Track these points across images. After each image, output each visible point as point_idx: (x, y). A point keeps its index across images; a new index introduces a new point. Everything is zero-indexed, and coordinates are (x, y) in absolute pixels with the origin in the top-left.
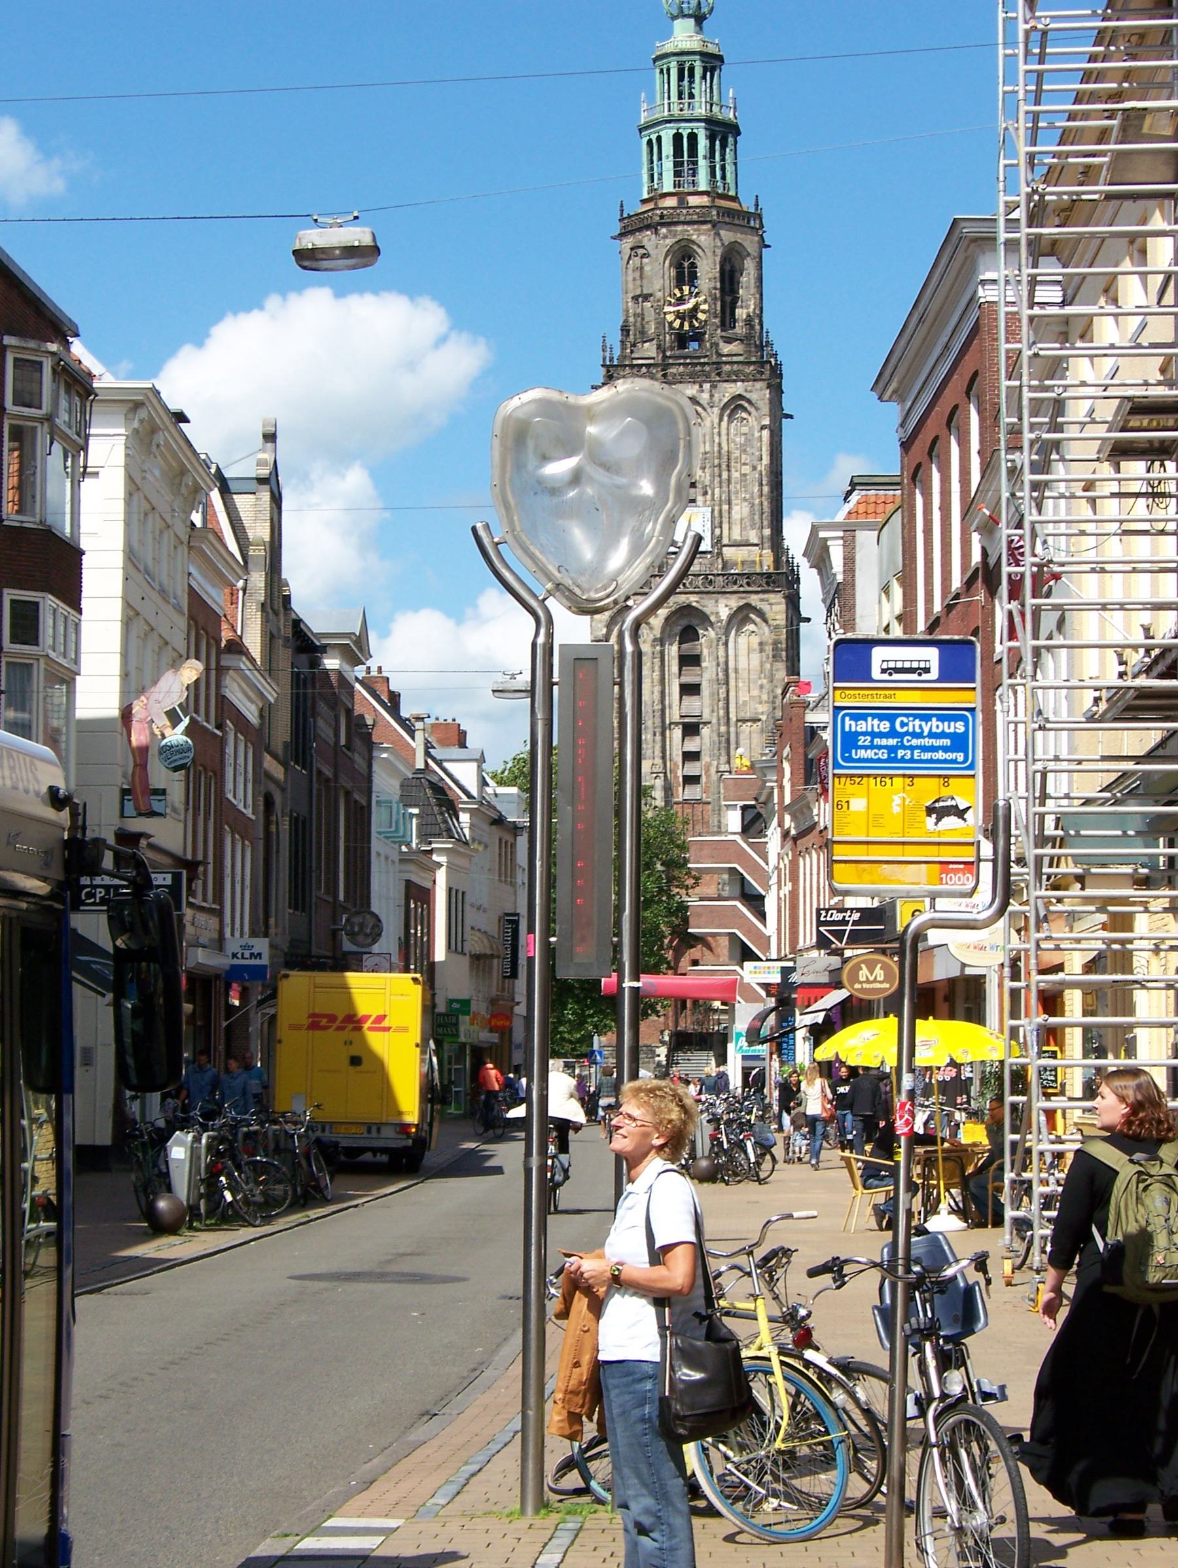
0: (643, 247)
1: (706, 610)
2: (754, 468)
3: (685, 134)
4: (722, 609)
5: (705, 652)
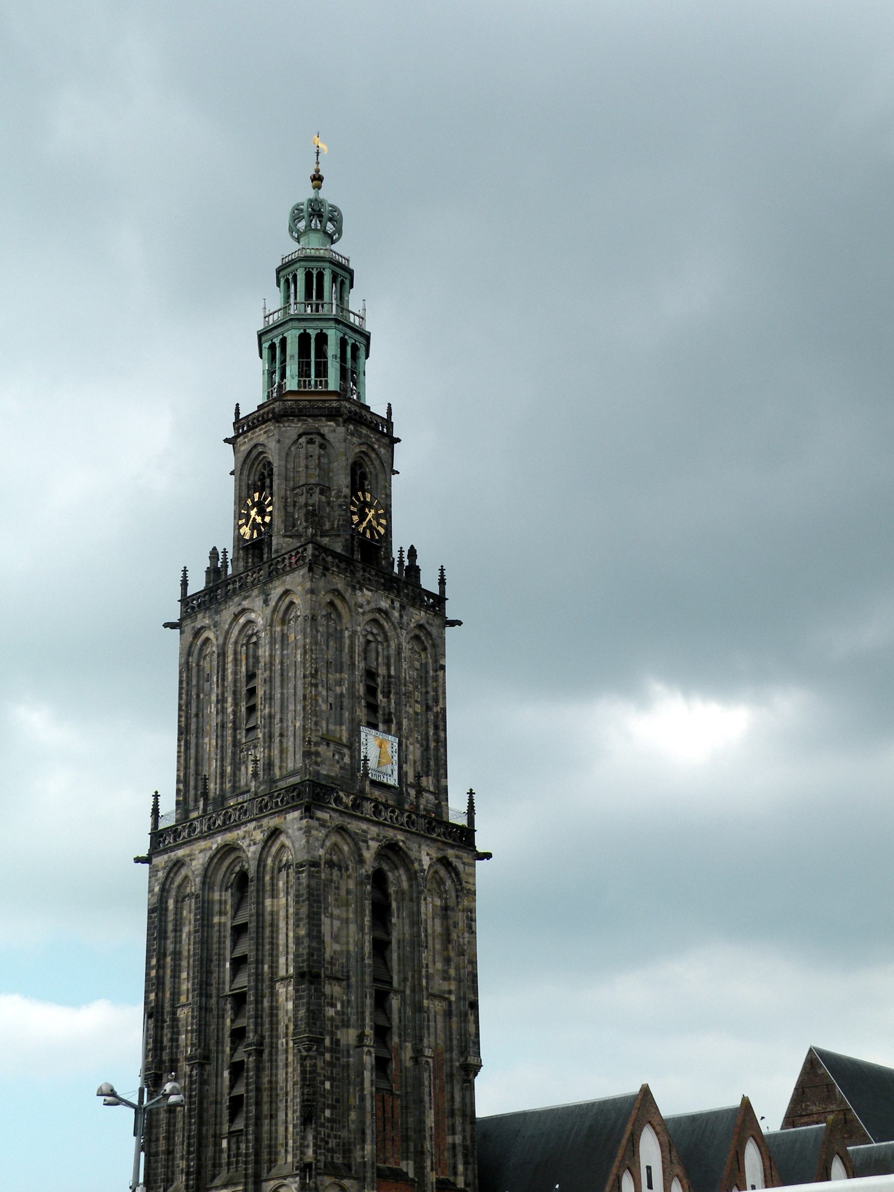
0: (322, 436)
1: (410, 853)
2: (428, 708)
3: (350, 341)
4: (425, 856)
5: (394, 905)
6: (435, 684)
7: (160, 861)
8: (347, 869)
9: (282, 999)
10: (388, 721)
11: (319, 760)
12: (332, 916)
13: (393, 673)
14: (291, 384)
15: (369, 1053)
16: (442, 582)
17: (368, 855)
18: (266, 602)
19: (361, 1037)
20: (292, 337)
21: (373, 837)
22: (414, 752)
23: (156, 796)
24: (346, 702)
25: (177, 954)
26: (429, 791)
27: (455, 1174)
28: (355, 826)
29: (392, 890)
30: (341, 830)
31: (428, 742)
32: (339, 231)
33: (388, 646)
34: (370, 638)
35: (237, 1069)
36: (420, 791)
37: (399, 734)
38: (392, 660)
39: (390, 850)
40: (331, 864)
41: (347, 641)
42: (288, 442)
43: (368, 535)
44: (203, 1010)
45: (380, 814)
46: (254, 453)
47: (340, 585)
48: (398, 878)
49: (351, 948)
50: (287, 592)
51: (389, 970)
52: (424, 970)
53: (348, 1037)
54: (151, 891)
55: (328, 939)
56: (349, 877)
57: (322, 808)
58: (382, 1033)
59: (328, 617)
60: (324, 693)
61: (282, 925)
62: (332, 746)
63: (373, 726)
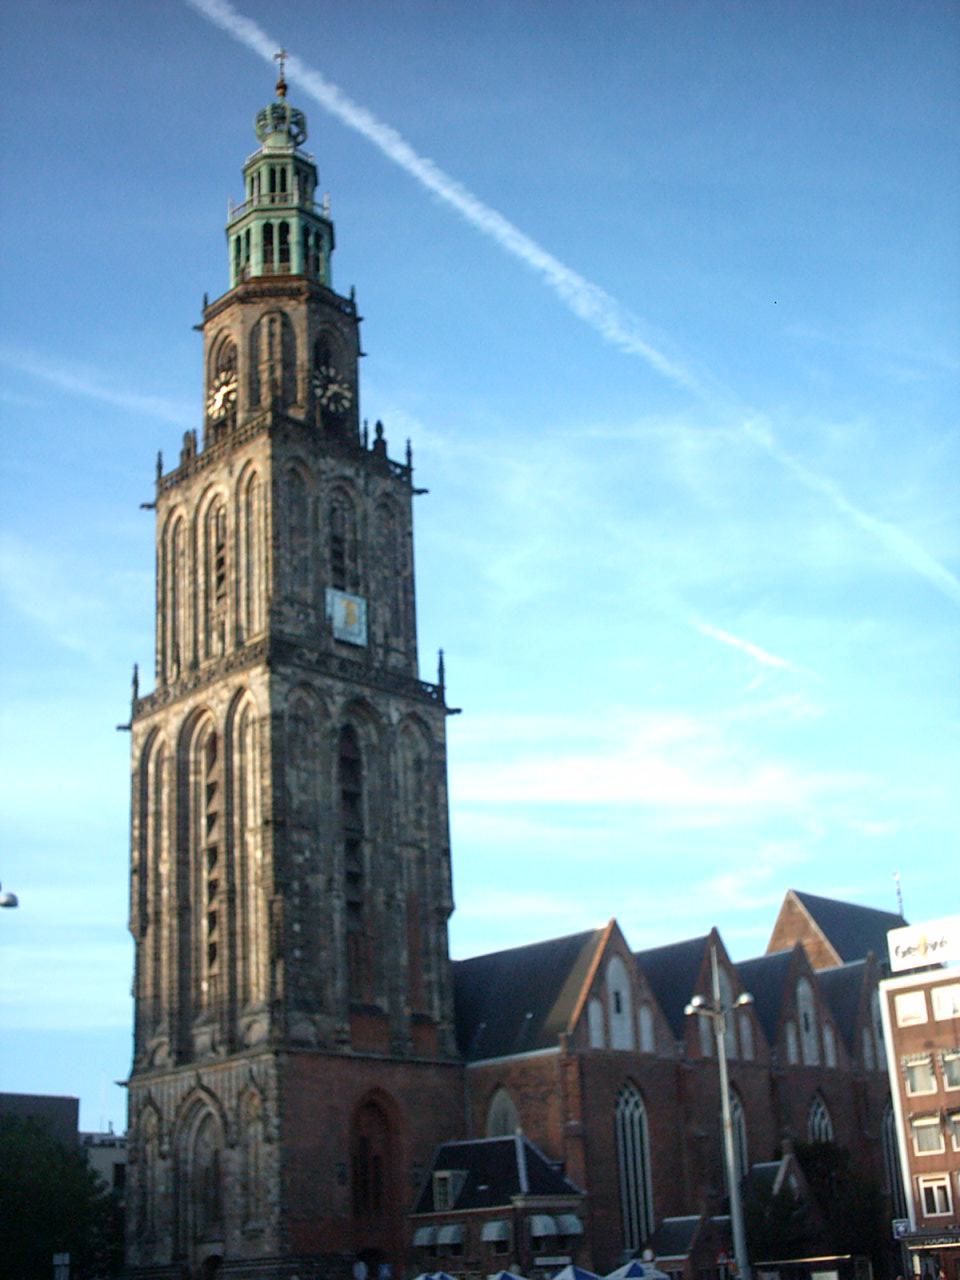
0: (284, 315)
3: (314, 230)
4: (395, 711)
5: (364, 758)
6: (403, 550)
7: (141, 727)
8: (313, 722)
9: (251, 848)
10: (355, 584)
11: (282, 619)
12: (298, 768)
13: (359, 537)
14: (255, 269)
15: (338, 897)
16: (409, 454)
17: (334, 709)
18: (231, 473)
19: (331, 880)
20: (256, 227)
21: (338, 694)
22: (384, 615)
23: (136, 668)
24: (310, 564)
25: (158, 814)
26: (397, 651)
27: (431, 1007)
28: (319, 682)
29: (362, 744)
30: (306, 685)
31: (397, 605)
32: (303, 131)
33: (355, 513)
34: (336, 505)
35: (213, 918)
36: (388, 649)
37: (367, 595)
38: (358, 526)
39: (357, 705)
40: (295, 718)
41: (310, 508)
42: (253, 322)
43: (332, 407)
44: (182, 863)
45: (346, 671)
46: (221, 337)
47: (302, 453)
48: (368, 735)
49: (319, 799)
50: (249, 462)
51: (359, 819)
52: (394, 820)
53: (318, 882)
54: (133, 756)
55: (294, 790)
56: (315, 731)
57: (285, 664)
58: (354, 878)
59: (291, 484)
60: (288, 556)
61: (250, 778)
62: (296, 607)
63: (342, 588)
